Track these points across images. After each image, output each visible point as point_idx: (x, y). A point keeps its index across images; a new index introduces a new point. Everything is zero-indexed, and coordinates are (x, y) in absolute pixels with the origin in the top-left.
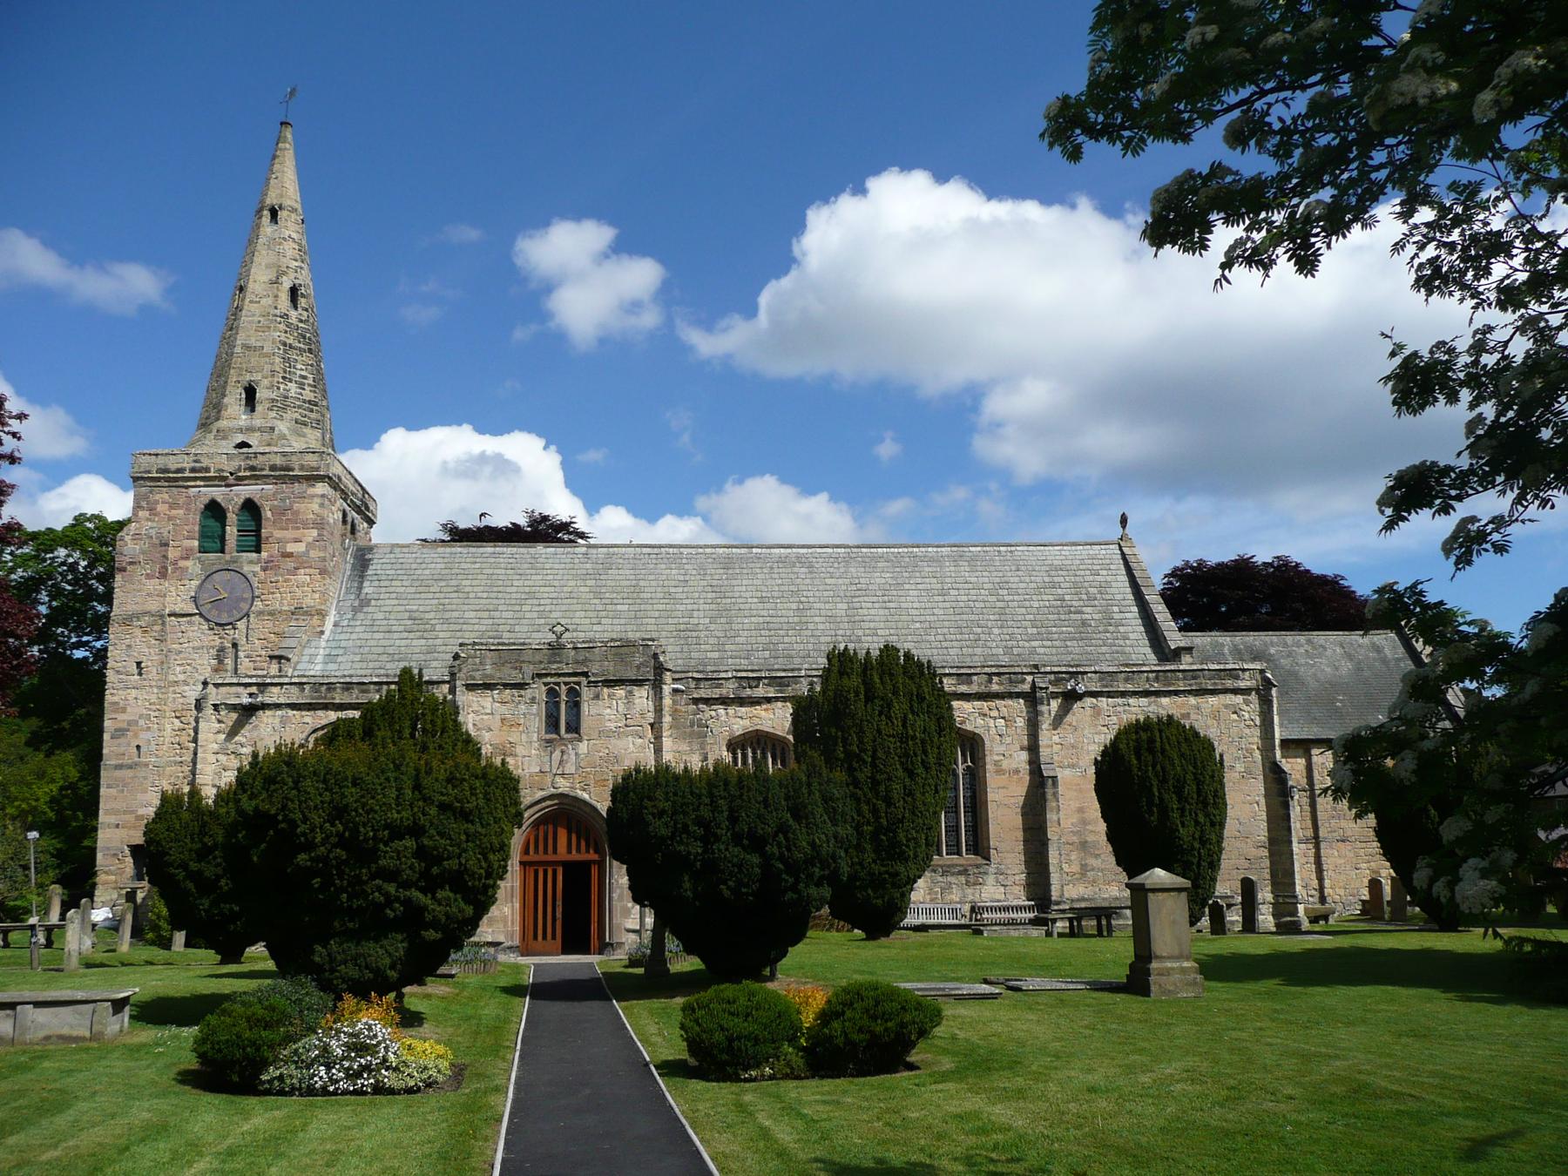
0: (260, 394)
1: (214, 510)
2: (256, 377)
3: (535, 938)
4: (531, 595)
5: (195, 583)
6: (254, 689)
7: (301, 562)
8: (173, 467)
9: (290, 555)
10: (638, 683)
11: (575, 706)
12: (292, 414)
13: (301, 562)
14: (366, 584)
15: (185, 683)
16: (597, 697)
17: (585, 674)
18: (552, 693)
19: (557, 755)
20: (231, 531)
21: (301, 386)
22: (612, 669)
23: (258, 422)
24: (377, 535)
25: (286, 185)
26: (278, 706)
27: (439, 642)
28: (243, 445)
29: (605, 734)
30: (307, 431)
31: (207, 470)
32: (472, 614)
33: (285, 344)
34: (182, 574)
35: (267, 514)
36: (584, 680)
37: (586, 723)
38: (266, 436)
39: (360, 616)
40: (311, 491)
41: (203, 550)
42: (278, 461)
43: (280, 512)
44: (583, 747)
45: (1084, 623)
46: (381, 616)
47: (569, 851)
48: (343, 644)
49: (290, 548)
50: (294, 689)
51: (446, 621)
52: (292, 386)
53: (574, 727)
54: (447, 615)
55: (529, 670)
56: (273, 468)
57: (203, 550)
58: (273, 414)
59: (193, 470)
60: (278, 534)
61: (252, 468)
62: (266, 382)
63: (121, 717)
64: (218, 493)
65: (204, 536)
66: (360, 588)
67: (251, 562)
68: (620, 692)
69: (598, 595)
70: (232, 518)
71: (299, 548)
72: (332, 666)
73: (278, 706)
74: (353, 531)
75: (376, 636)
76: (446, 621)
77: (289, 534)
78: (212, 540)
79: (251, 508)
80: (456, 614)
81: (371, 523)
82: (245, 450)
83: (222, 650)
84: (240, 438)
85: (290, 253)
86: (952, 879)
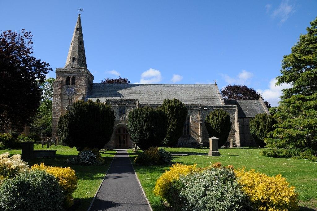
14: (92, 90)
23: (75, 64)
24: (95, 82)
31: (67, 71)
45: (208, 98)
52: (81, 58)
53: (124, 113)
59: (65, 71)
64: (68, 75)
66: (91, 90)
70: (71, 79)
71: (82, 84)
74: (90, 81)
81: (93, 79)
83: (70, 100)
86: (185, 139)
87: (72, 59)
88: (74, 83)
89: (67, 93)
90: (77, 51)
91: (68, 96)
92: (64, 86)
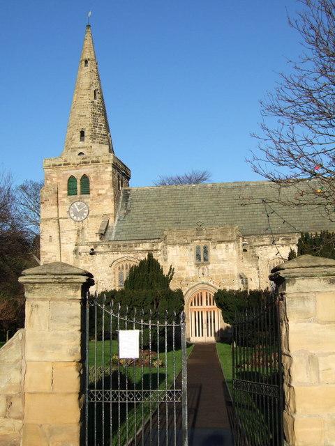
0: (86, 134)
1: (72, 180)
2: (84, 127)
3: (196, 336)
4: (191, 205)
5: (68, 207)
6: (92, 247)
7: (105, 196)
8: (57, 163)
9: (99, 195)
10: (230, 241)
11: (206, 252)
12: (97, 140)
13: (105, 196)
15: (67, 244)
16: (215, 248)
17: (210, 240)
18: (198, 248)
19: (201, 270)
20: (79, 186)
21: (100, 129)
22: (220, 237)
25: (88, 43)
26: (101, 253)
27: (157, 225)
28: (81, 154)
29: (219, 261)
30: (103, 146)
31: (69, 164)
32: (168, 214)
33: (93, 113)
34: (64, 204)
35: (91, 179)
36: (210, 242)
37: (211, 260)
38: (89, 150)
39: (127, 216)
40: (106, 170)
41: (69, 194)
42: (94, 159)
43: (96, 178)
44: (210, 267)
46: (135, 216)
47: (207, 304)
48: (122, 228)
49: (100, 192)
50: (106, 246)
51: (159, 217)
53: (205, 260)
54: (159, 215)
55: (189, 239)
56: (92, 162)
57: (69, 194)
58: (91, 141)
59: (64, 165)
60: (96, 187)
61: (85, 163)
62: (87, 129)
63: (46, 257)
65: (69, 189)
67: (86, 197)
68: (223, 245)
69: (217, 204)
70: (79, 181)
72: (117, 236)
73: (101, 253)
75: (134, 224)
76: (159, 217)
77: (99, 187)
78: (71, 190)
79: (85, 179)
80: (162, 214)
81: (129, 178)
82: (82, 156)
83: (79, 231)
84: (81, 151)
85: (93, 77)
87: (79, 134)
88: (86, 190)
89: (72, 215)
90: (88, 115)
91: (75, 221)
92: (63, 200)
